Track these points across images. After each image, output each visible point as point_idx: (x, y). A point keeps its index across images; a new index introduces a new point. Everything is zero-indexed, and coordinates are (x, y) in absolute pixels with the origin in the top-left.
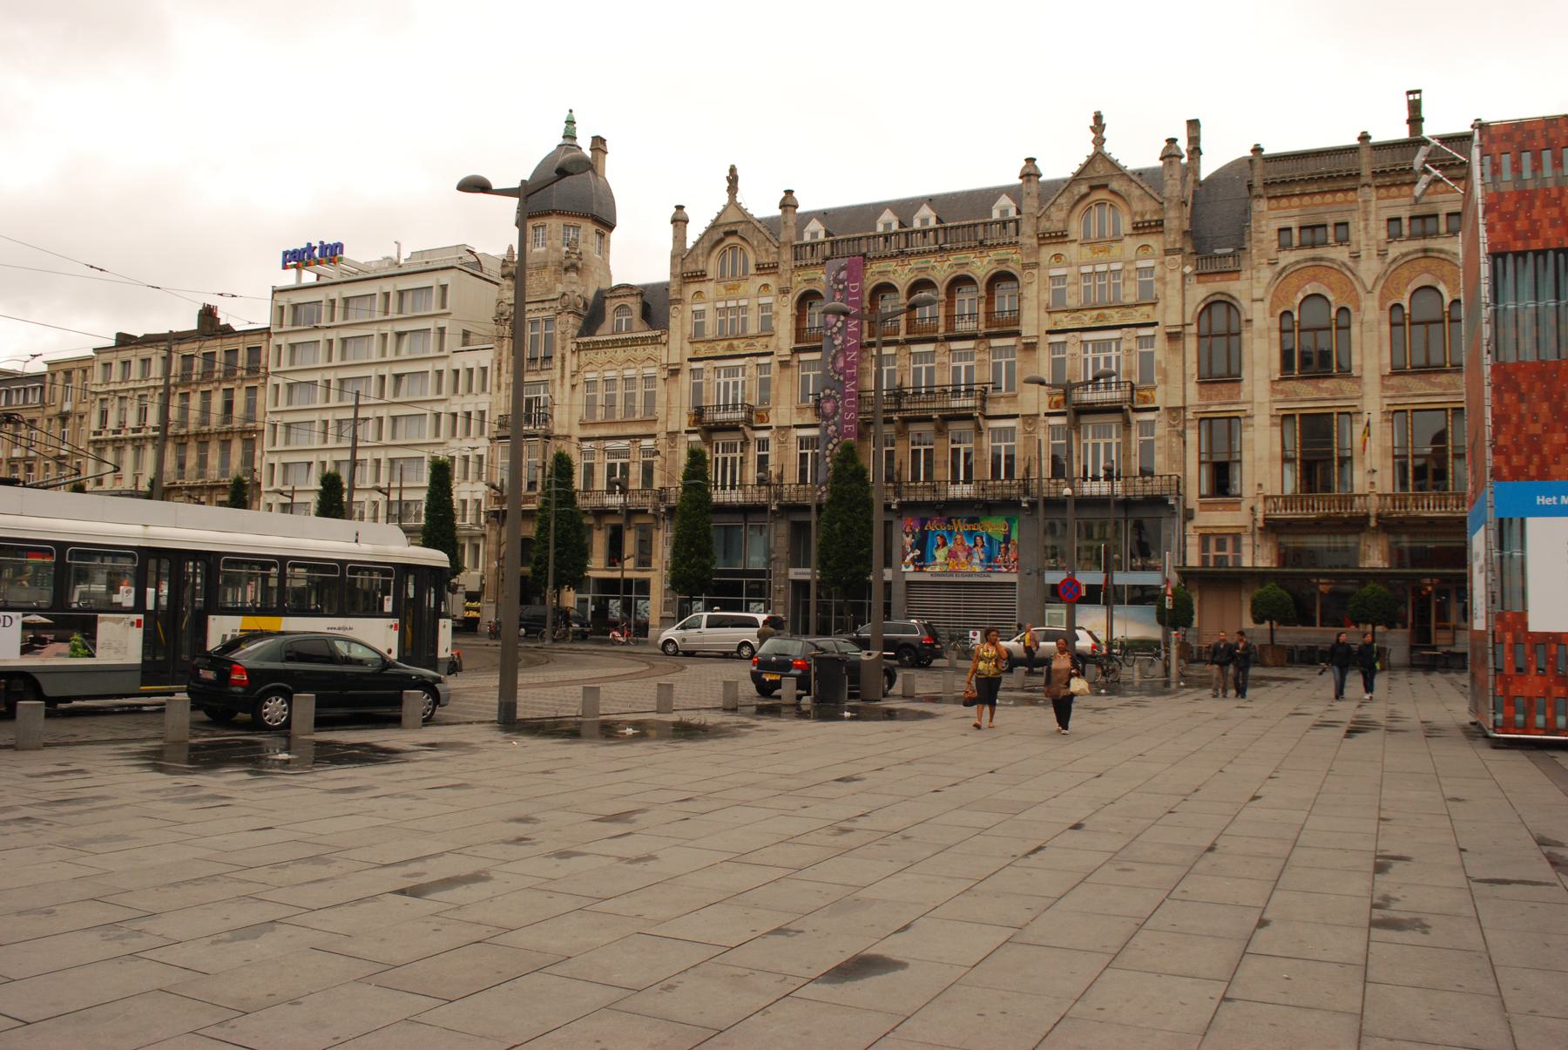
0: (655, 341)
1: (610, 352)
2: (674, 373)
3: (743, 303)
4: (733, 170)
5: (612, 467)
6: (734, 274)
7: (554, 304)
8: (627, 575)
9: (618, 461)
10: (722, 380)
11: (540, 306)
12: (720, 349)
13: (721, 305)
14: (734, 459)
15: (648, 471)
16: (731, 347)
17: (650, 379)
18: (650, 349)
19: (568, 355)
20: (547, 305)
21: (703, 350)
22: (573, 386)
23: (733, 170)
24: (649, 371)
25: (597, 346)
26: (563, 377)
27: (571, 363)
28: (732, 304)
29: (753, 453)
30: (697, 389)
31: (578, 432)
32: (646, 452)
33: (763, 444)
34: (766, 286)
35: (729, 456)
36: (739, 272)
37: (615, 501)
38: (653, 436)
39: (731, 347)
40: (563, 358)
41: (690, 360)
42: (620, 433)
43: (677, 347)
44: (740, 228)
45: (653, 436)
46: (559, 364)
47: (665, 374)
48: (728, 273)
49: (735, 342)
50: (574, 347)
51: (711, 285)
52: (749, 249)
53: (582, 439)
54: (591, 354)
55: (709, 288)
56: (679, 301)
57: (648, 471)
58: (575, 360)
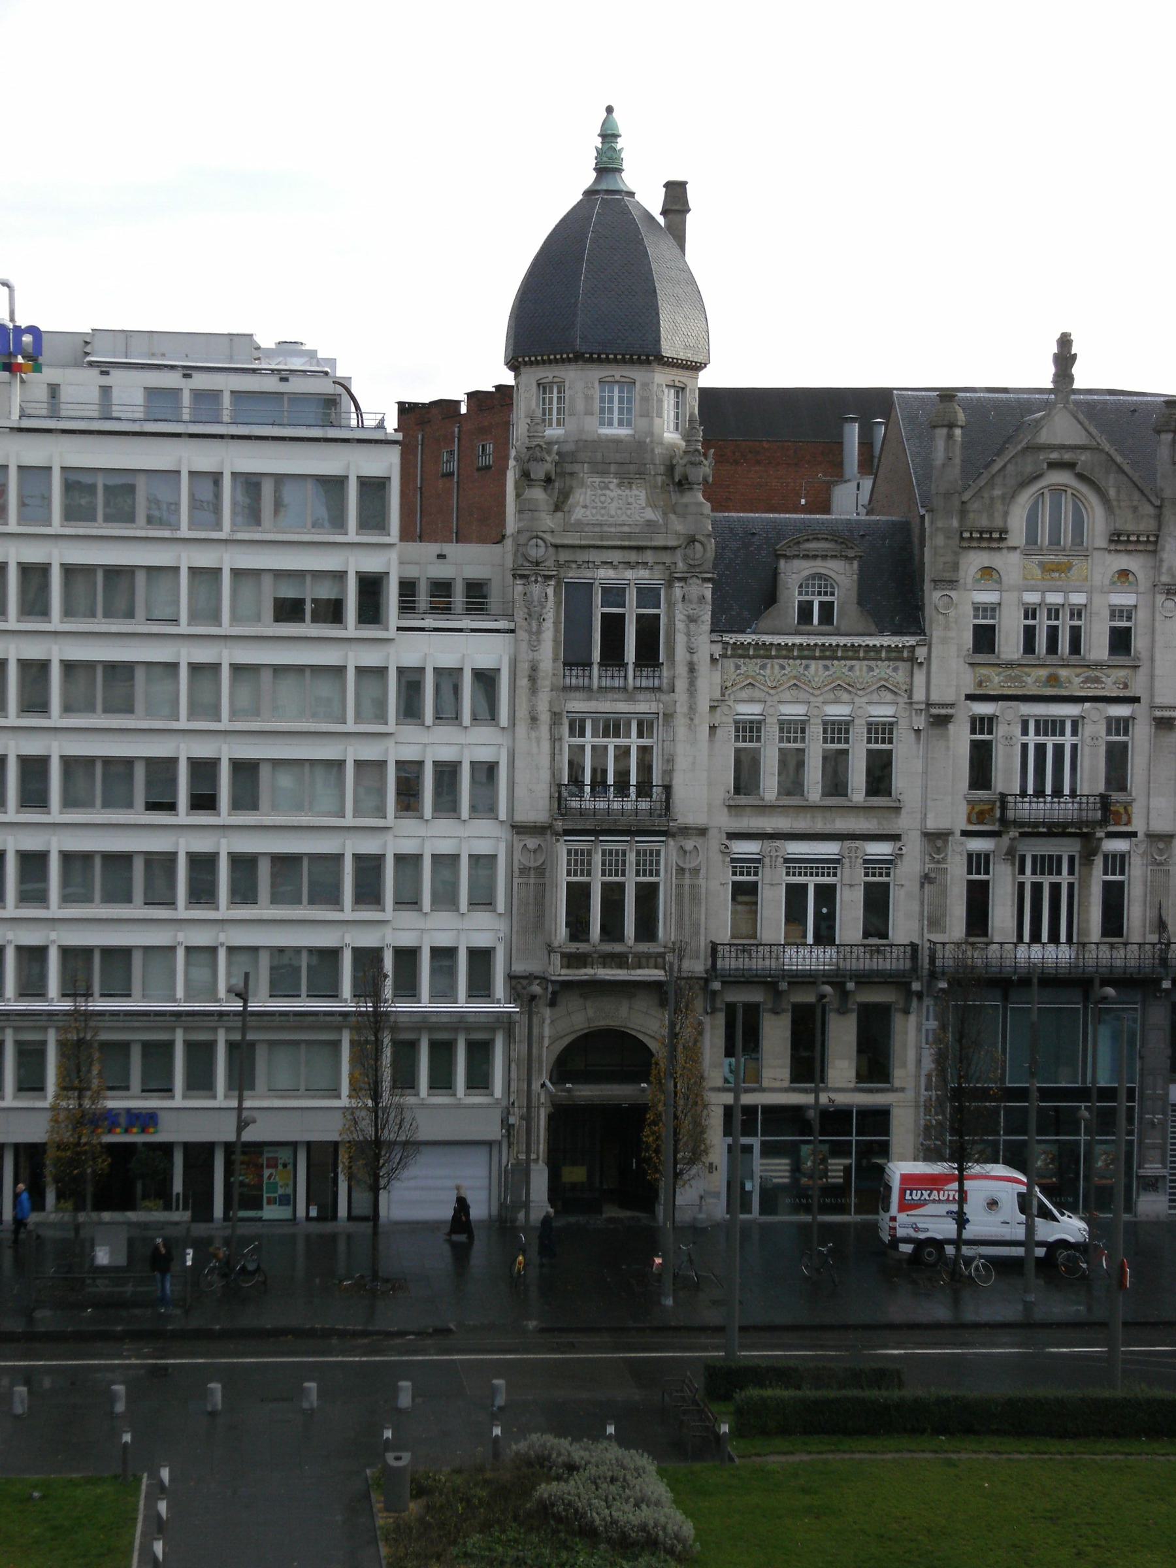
0: (895, 654)
1: (794, 667)
2: (941, 721)
3: (1078, 599)
4: (1065, 341)
5: (796, 894)
6: (1055, 540)
7: (667, 558)
8: (842, 1099)
9: (811, 882)
10: (1032, 739)
11: (633, 557)
12: (1033, 680)
13: (1032, 598)
14: (1055, 887)
15: (877, 902)
16: (1053, 680)
17: (881, 730)
18: (883, 669)
19: (704, 666)
20: (649, 557)
21: (996, 682)
22: (713, 728)
23: (1065, 341)
24: (883, 711)
25: (764, 652)
26: (692, 708)
27: (709, 682)
28: (1054, 598)
29: (1098, 877)
30: (981, 757)
31: (725, 822)
32: (872, 865)
33: (1117, 862)
34: (1124, 573)
35: (1046, 880)
36: (1067, 538)
37: (809, 958)
38: (895, 838)
39: (1053, 680)
40: (692, 668)
41: (969, 697)
42: (819, 826)
43: (949, 670)
44: (1083, 457)
45: (895, 838)
46: (681, 685)
47: (920, 722)
48: (1044, 538)
49: (1063, 673)
50: (717, 650)
51: (1015, 558)
52: (1093, 499)
53: (733, 836)
54: (751, 667)
55: (1009, 563)
56: (952, 583)
57: (877, 902)
58: (717, 678)
